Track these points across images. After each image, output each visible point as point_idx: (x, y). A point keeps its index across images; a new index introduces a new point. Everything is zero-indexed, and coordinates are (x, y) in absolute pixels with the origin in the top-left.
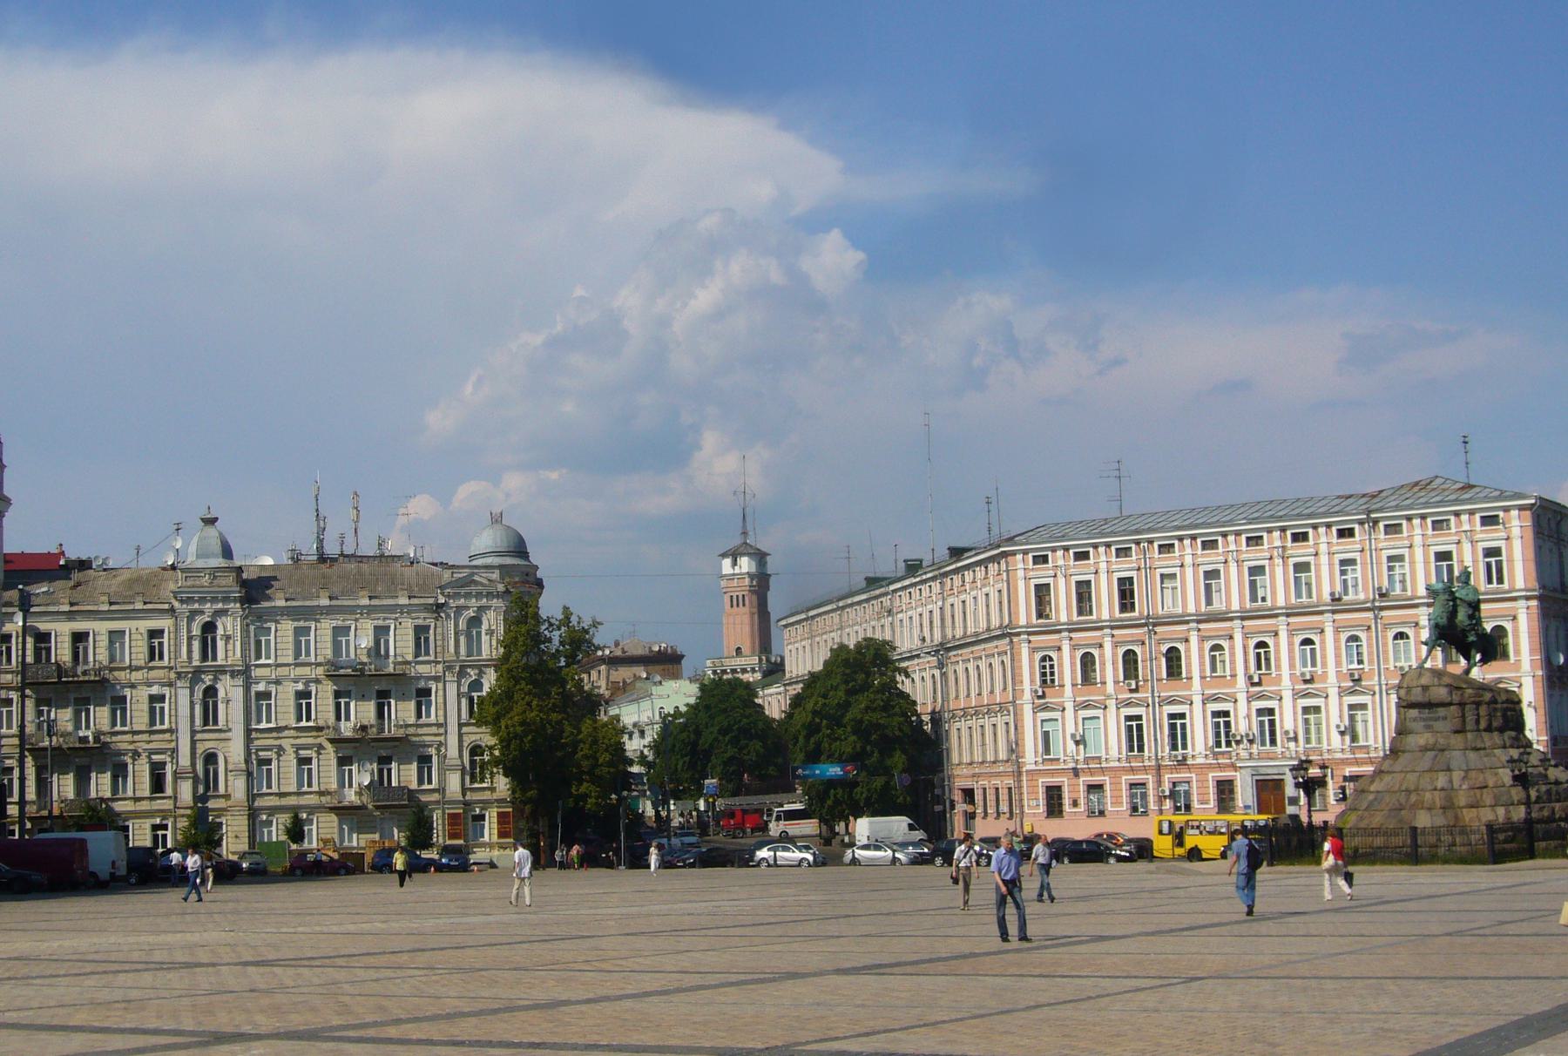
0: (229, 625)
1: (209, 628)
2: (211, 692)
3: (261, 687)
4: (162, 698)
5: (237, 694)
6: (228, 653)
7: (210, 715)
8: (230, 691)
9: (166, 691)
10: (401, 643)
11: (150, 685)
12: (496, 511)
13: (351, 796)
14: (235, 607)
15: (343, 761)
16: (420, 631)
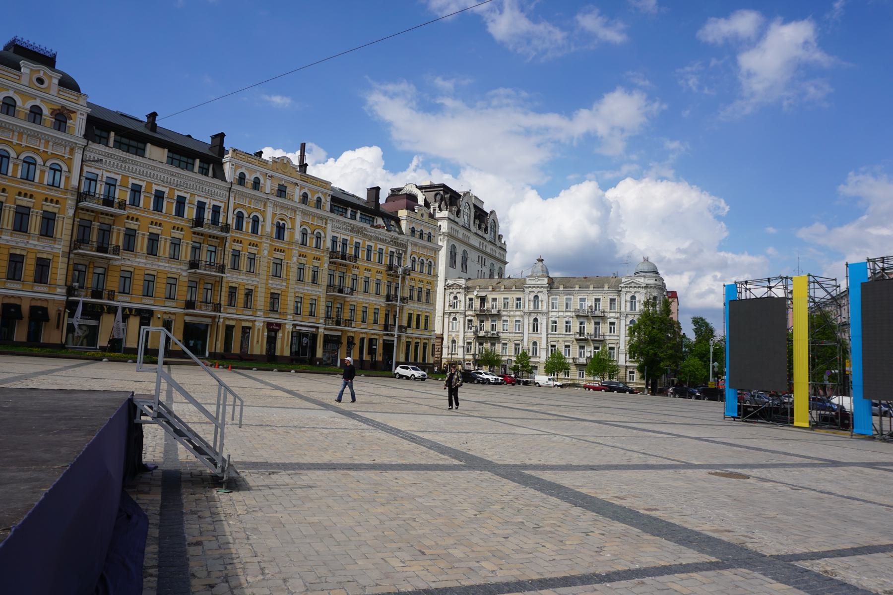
0: (543, 297)
1: (536, 297)
2: (536, 320)
3: (553, 319)
4: (519, 321)
5: (544, 321)
6: (543, 307)
7: (535, 329)
8: (542, 320)
9: (521, 319)
10: (604, 305)
11: (515, 316)
12: (646, 257)
13: (582, 360)
14: (545, 290)
15: (582, 347)
16: (612, 300)
